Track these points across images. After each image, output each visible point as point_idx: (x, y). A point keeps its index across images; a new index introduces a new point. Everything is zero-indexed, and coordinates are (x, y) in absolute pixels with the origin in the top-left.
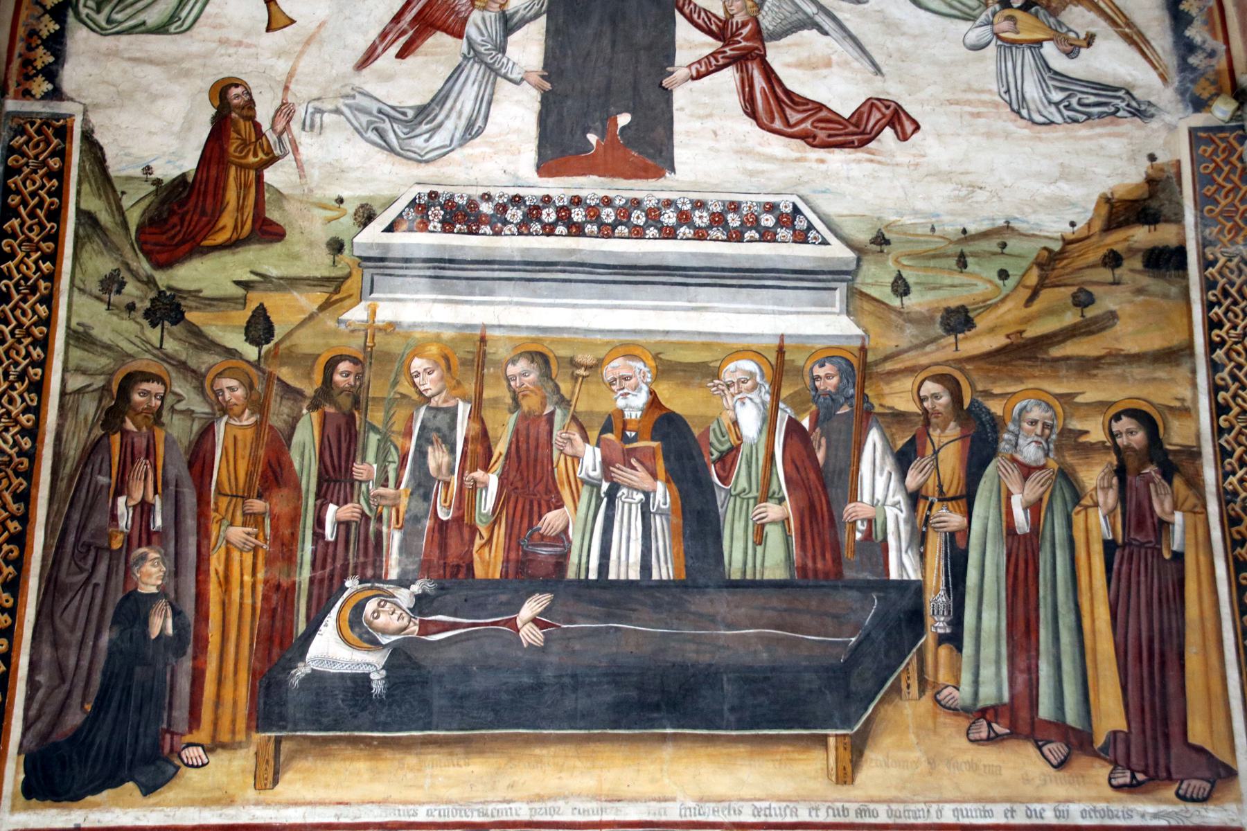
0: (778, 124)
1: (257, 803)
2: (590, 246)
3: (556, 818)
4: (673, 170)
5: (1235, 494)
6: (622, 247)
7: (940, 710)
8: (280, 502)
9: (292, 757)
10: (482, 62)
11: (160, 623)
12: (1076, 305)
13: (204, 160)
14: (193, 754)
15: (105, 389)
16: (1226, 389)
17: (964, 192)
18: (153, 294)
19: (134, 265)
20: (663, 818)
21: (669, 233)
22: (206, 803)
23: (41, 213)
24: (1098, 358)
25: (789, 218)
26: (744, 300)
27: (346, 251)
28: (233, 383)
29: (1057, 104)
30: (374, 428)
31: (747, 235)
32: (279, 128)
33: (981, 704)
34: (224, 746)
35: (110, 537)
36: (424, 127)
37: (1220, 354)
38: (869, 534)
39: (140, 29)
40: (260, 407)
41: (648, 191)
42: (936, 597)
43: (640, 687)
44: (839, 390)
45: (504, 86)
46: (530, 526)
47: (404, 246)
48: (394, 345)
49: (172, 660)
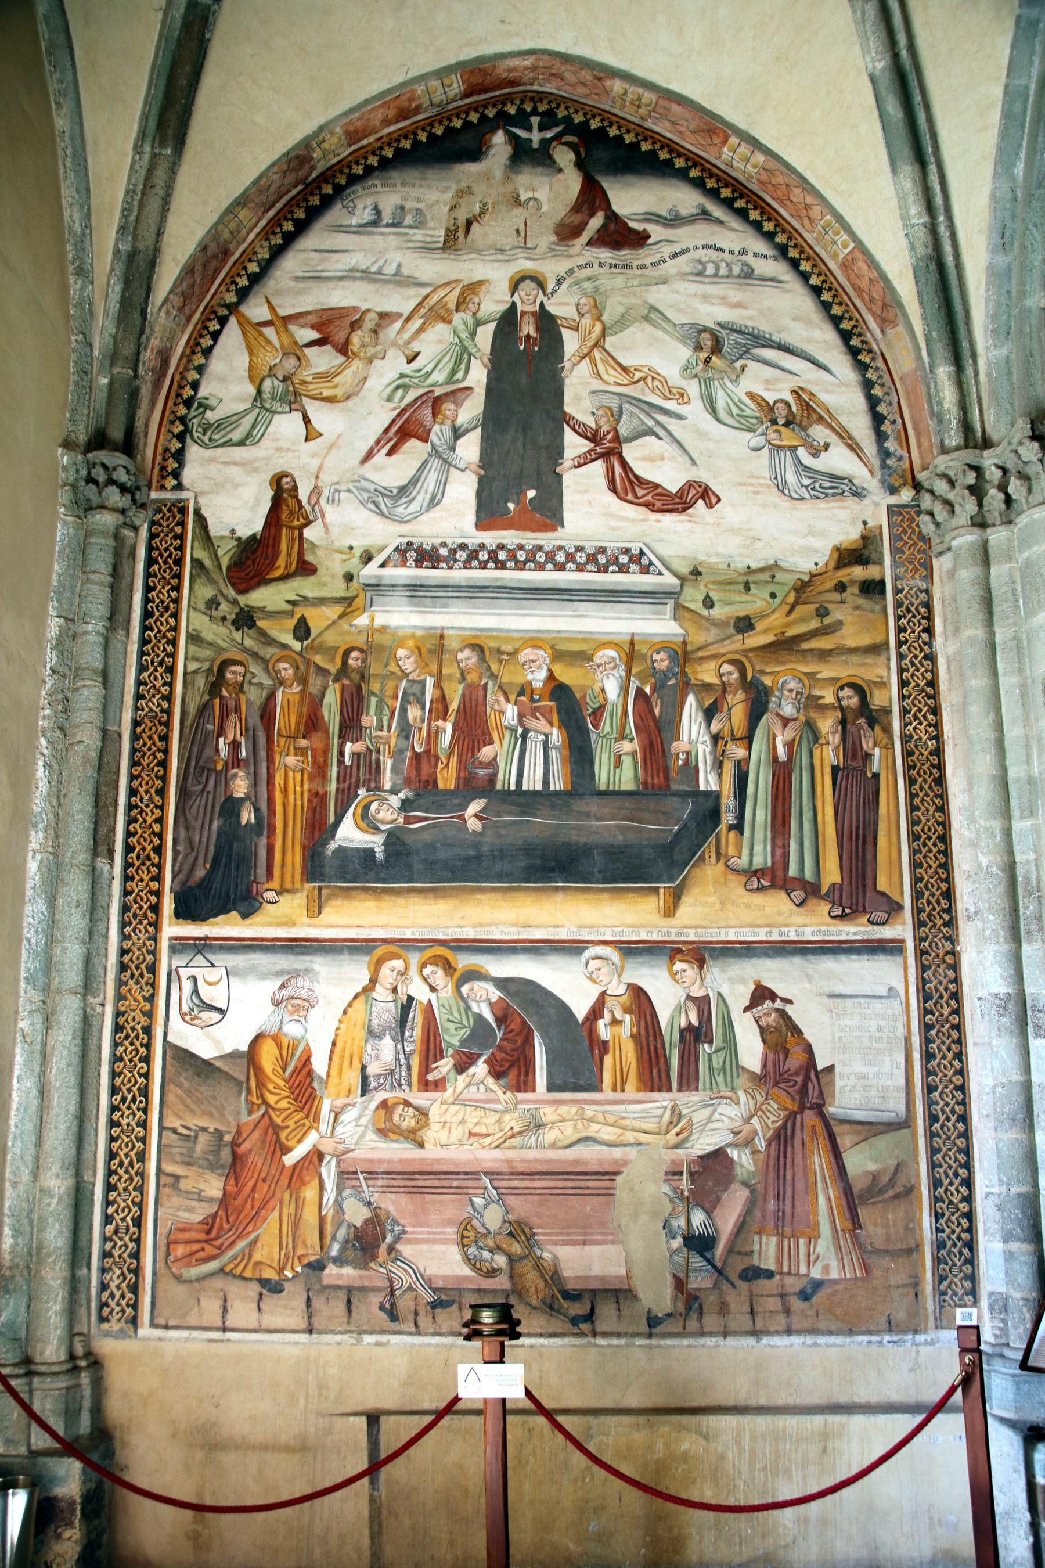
0: (630, 497)
1: (309, 926)
2: (510, 576)
3: (491, 937)
4: (563, 526)
6: (530, 577)
7: (729, 872)
8: (317, 741)
9: (328, 899)
10: (440, 457)
11: (247, 816)
12: (818, 616)
13: (267, 524)
14: (270, 895)
16: (908, 671)
17: (749, 542)
18: (237, 610)
19: (225, 592)
20: (557, 938)
21: (561, 567)
22: (279, 925)
23: (170, 561)
24: (831, 650)
25: (637, 558)
27: (355, 580)
28: (286, 665)
29: (806, 487)
30: (373, 694)
31: (611, 569)
33: (754, 868)
34: (288, 891)
35: (215, 763)
36: (404, 500)
38: (687, 762)
39: (229, 443)
40: (303, 681)
41: (547, 540)
42: (728, 801)
43: (543, 857)
44: (669, 669)
46: (473, 756)
47: (392, 576)
48: (386, 640)
49: (255, 838)
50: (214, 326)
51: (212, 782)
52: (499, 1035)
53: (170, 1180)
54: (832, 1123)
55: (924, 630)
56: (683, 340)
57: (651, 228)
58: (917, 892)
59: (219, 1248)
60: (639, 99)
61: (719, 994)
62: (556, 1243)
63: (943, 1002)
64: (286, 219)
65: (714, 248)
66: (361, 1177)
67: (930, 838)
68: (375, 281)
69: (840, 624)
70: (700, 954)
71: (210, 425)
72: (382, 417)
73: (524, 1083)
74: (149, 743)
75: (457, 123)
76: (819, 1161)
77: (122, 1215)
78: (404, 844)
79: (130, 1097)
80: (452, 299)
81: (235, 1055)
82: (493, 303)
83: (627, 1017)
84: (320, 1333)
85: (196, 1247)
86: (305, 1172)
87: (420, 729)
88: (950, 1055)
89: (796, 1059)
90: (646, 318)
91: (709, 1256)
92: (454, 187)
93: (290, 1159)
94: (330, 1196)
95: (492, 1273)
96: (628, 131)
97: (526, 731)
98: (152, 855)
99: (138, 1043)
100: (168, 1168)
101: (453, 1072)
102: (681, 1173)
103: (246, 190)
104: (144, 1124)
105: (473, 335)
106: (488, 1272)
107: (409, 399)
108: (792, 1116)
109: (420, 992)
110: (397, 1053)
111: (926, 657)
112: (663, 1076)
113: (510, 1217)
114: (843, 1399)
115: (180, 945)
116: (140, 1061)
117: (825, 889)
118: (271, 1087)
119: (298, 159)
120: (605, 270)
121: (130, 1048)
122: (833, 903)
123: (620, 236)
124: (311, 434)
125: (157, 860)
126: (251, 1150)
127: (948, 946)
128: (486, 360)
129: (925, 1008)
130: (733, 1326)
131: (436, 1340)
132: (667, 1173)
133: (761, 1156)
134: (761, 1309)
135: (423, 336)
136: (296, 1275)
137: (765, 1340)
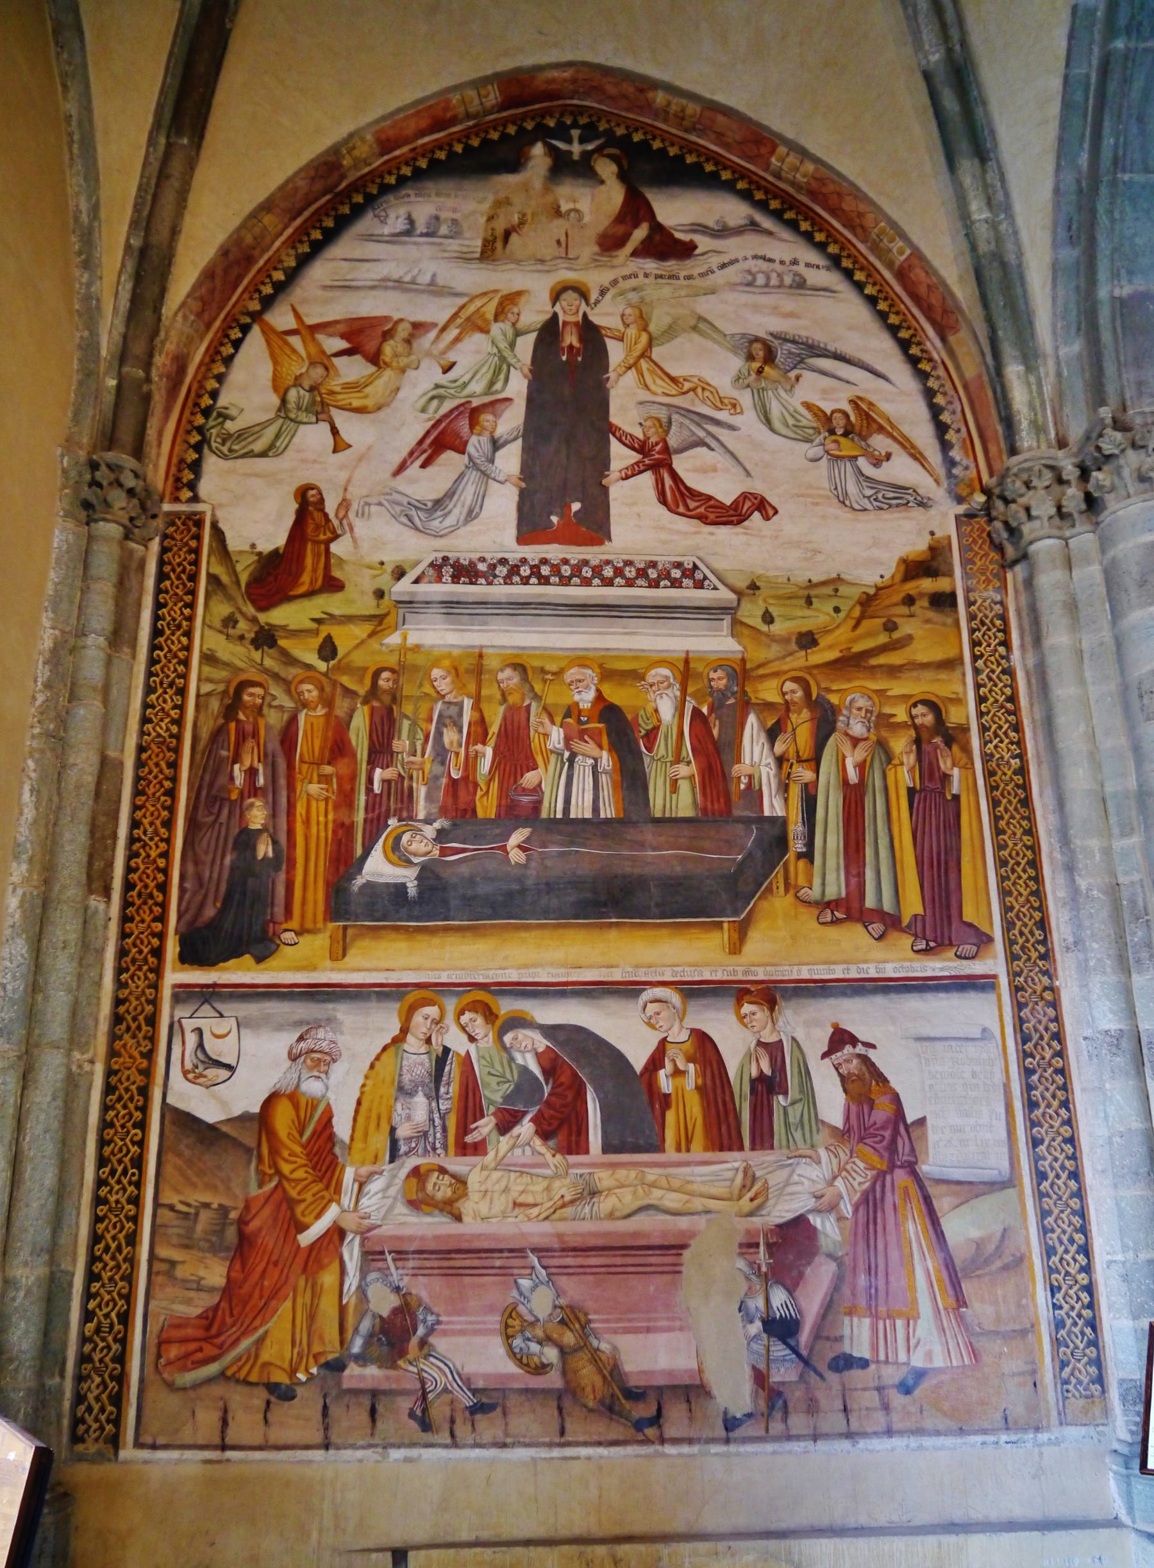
0: (681, 509)
1: (332, 970)
2: (554, 592)
4: (610, 539)
5: (992, 755)
7: (798, 903)
8: (343, 766)
9: (355, 937)
10: (478, 469)
11: (264, 849)
14: (288, 936)
15: (225, 692)
16: (985, 686)
18: (256, 628)
19: (244, 609)
21: (608, 582)
22: (299, 969)
25: (690, 572)
26: (663, 627)
27: (386, 597)
28: (310, 687)
32: (341, 515)
33: (827, 899)
34: (309, 931)
35: (230, 792)
36: (439, 513)
37: (980, 663)
38: (749, 785)
39: (250, 454)
40: (329, 703)
41: (593, 554)
42: (796, 828)
45: (493, 485)
46: (515, 781)
48: (420, 660)
50: (236, 334)
51: (225, 811)
52: (547, 1090)
53: (164, 1267)
54: (927, 1183)
55: (1001, 644)
56: (734, 350)
57: (697, 238)
58: (1008, 922)
59: (220, 1347)
60: (683, 110)
61: (793, 1039)
62: (615, 1332)
63: (1044, 1043)
64: (314, 228)
65: (764, 258)
66: (389, 1258)
67: (1018, 864)
68: (409, 290)
69: (909, 639)
70: (770, 995)
71: (230, 435)
72: (414, 429)
73: (575, 1143)
74: (155, 770)
75: (495, 136)
76: (914, 1228)
77: (105, 1311)
78: (438, 877)
79: (120, 1169)
80: (490, 310)
81: (245, 1118)
82: (534, 313)
83: (691, 1067)
84: (338, 1448)
85: (192, 1346)
86: (323, 1253)
87: (457, 754)
88: (1055, 1103)
89: (882, 1112)
90: (695, 328)
91: (792, 1342)
92: (491, 198)
93: (306, 1239)
94: (352, 1281)
95: (541, 1369)
96: (672, 145)
97: (573, 756)
98: (156, 893)
99: (131, 1106)
100: (163, 1252)
101: (495, 1134)
102: (757, 1245)
103: (272, 195)
104: (136, 1201)
105: (512, 345)
106: (537, 1367)
107: (444, 410)
108: (881, 1176)
109: (456, 1042)
110: (431, 1112)
111: (1004, 672)
112: (734, 1133)
113: (562, 1301)
114: (958, 1516)
115: (183, 994)
116: (135, 1126)
117: (906, 921)
118: (285, 1154)
119: (327, 166)
120: (652, 279)
121: (123, 1112)
122: (916, 936)
123: (666, 247)
124: (339, 445)
125: (160, 898)
126: (260, 1229)
127: (1046, 980)
128: (526, 371)
129: (1024, 1051)
130: (824, 1427)
131: (477, 1452)
132: (741, 1245)
133: (848, 1224)
134: (855, 1406)
135: (459, 346)
136: (311, 1377)
137: (862, 1443)
